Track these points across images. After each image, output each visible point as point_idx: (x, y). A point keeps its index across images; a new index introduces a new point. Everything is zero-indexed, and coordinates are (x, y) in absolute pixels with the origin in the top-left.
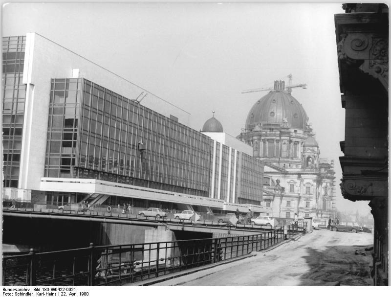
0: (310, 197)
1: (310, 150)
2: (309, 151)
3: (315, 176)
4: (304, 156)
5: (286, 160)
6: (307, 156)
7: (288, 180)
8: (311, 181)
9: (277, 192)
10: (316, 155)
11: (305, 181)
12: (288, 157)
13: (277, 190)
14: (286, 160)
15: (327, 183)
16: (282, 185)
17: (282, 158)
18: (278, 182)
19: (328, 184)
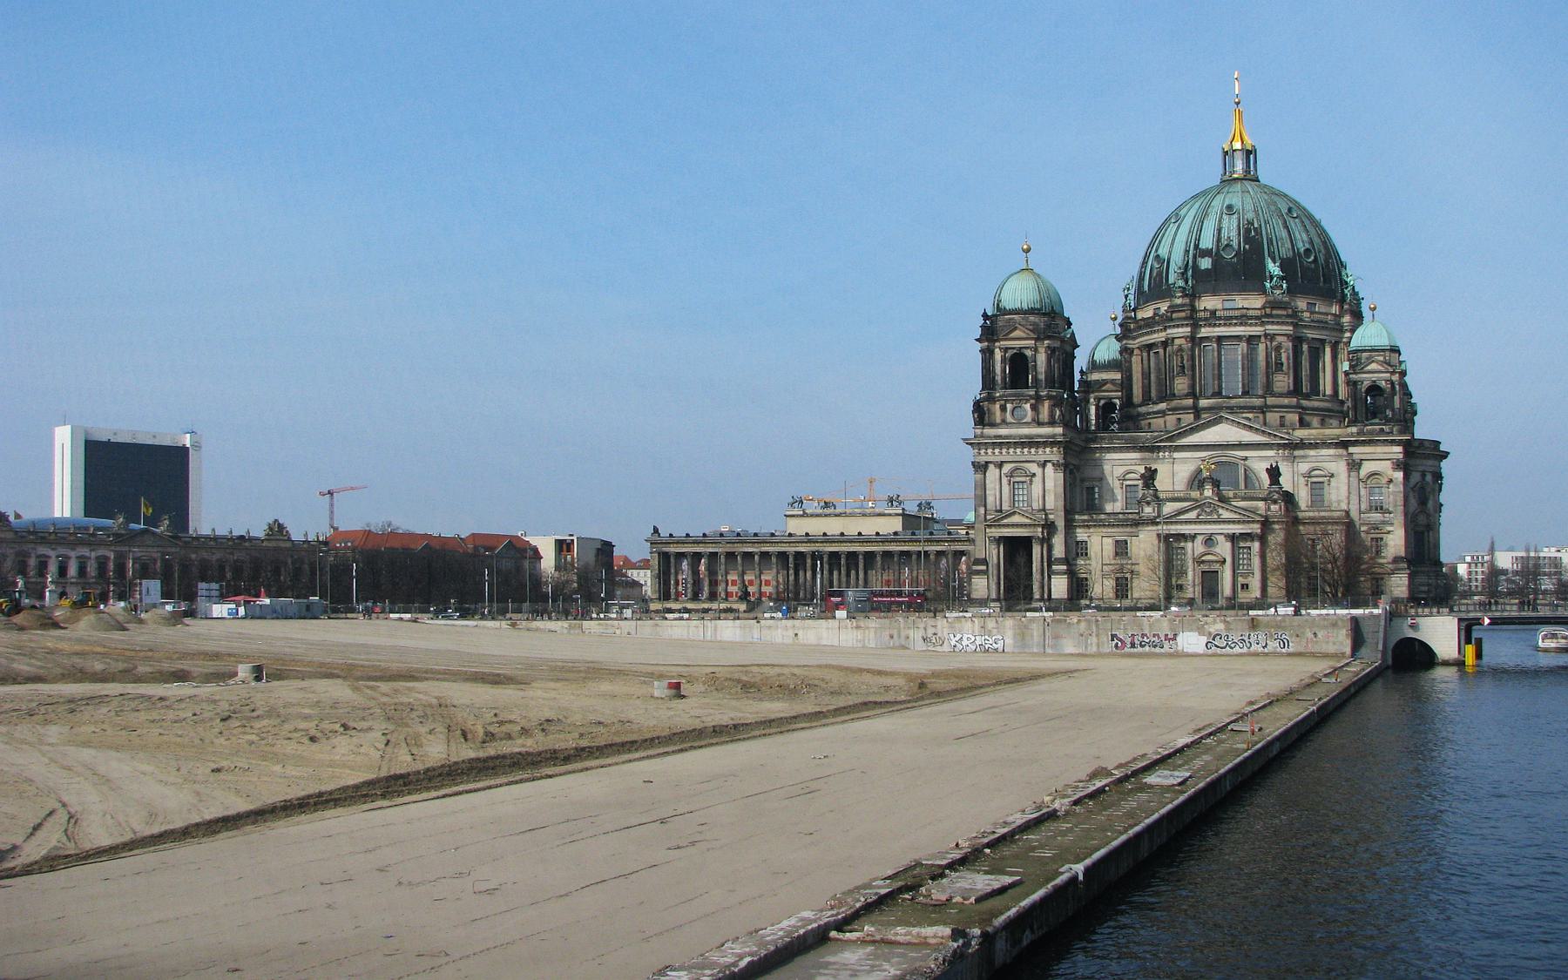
0: (1384, 523)
1: (1377, 362)
2: (1373, 366)
3: (1399, 449)
4: (1355, 383)
5: (1286, 401)
6: (1366, 384)
7: (1304, 467)
8: (1385, 467)
9: (1274, 507)
10: (1396, 378)
11: (1367, 468)
12: (1289, 394)
13: (1275, 502)
14: (1286, 401)
15: (1423, 475)
16: (1286, 482)
17: (1273, 395)
18: (1274, 473)
19: (1429, 478)
